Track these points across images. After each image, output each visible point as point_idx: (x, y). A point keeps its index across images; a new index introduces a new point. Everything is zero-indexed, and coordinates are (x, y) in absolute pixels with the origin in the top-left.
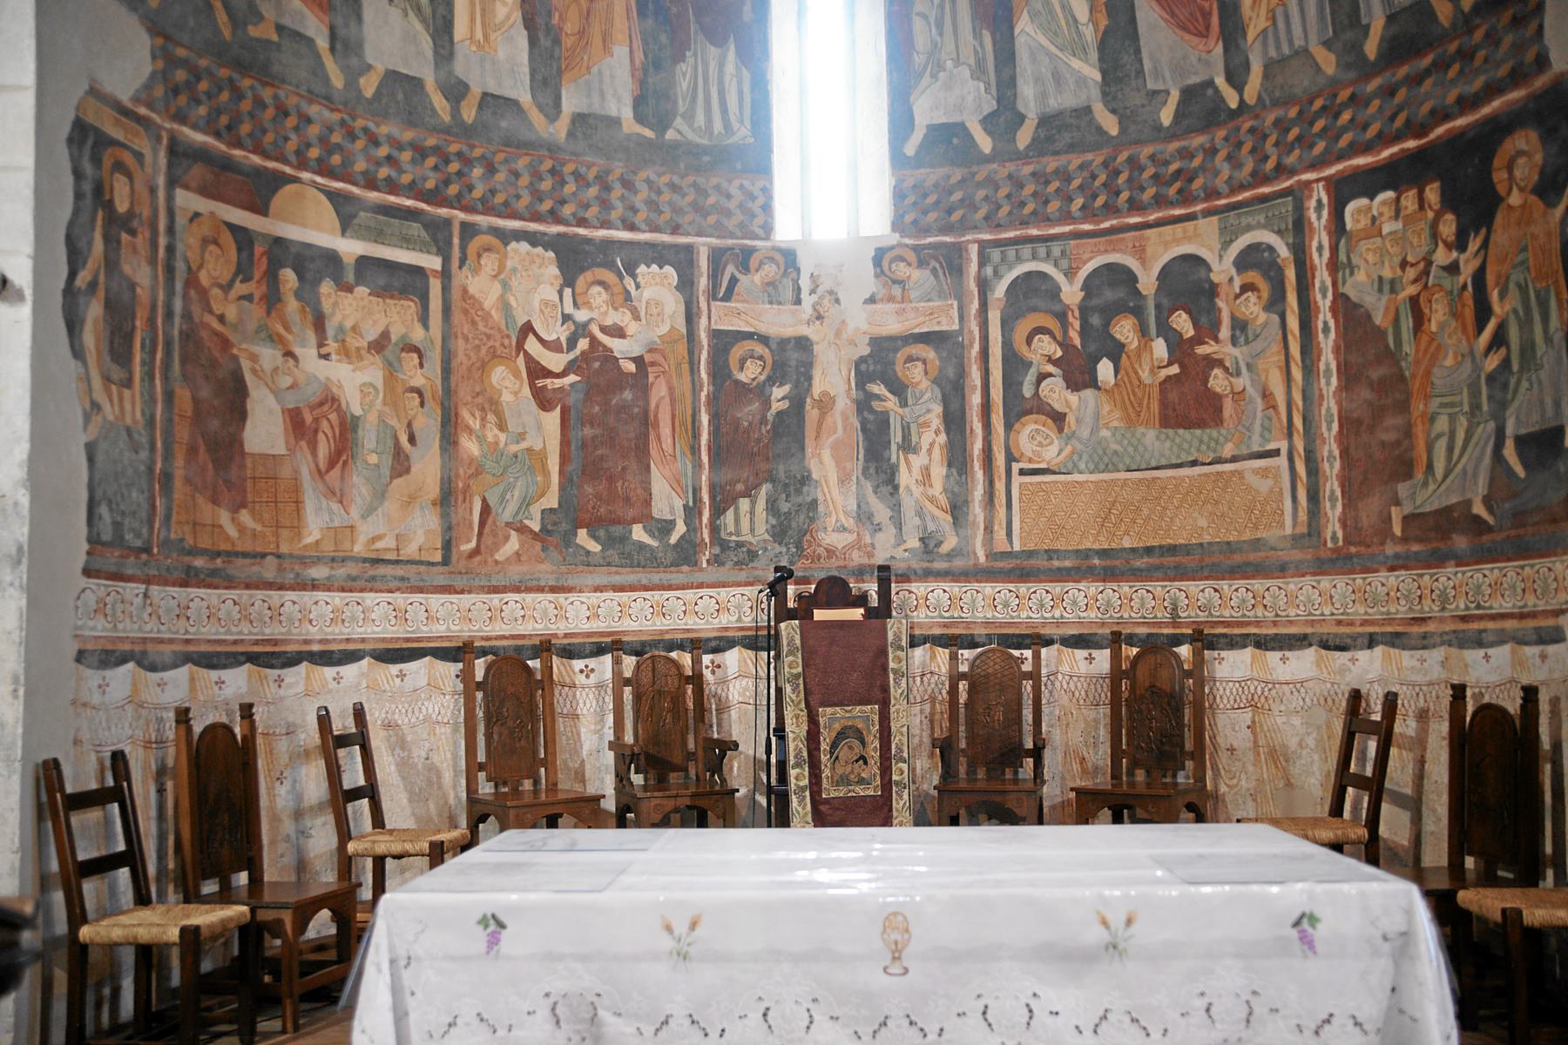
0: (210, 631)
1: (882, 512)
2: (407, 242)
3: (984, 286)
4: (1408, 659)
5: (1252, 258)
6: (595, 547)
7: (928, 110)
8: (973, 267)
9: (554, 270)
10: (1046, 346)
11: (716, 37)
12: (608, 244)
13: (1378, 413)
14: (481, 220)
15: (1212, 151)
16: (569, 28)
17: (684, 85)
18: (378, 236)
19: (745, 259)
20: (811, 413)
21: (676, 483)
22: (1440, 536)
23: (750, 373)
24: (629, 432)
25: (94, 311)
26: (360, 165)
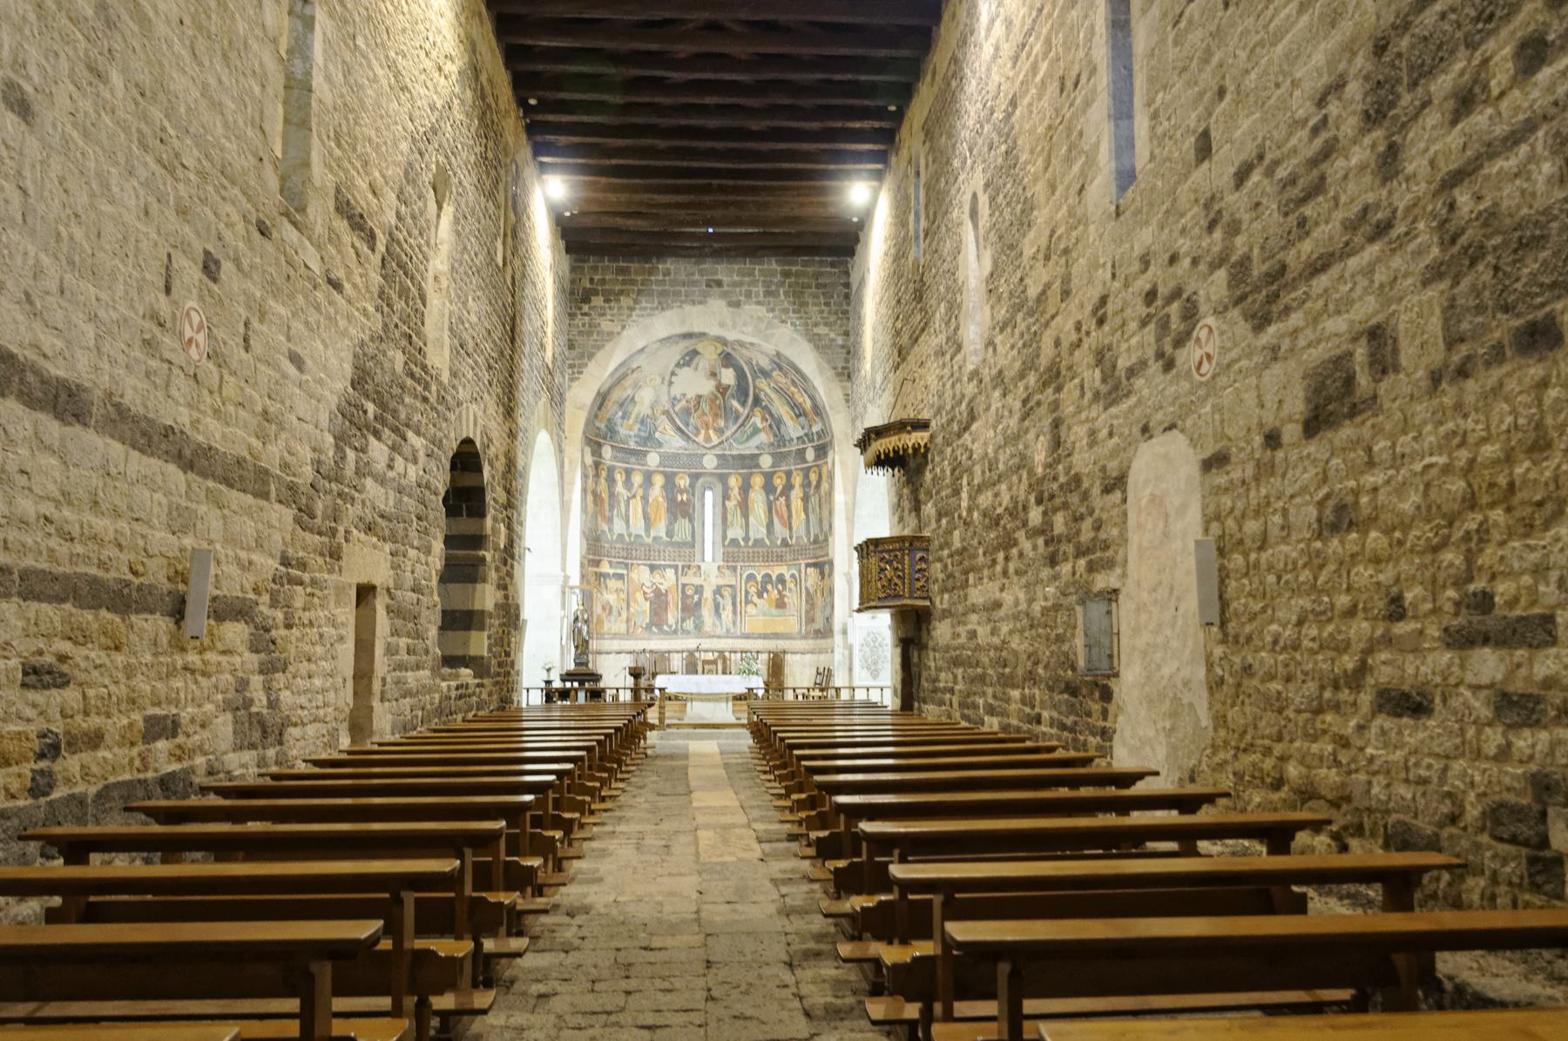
5: (793, 576)
7: (731, 534)
10: (753, 590)
23: (690, 592)
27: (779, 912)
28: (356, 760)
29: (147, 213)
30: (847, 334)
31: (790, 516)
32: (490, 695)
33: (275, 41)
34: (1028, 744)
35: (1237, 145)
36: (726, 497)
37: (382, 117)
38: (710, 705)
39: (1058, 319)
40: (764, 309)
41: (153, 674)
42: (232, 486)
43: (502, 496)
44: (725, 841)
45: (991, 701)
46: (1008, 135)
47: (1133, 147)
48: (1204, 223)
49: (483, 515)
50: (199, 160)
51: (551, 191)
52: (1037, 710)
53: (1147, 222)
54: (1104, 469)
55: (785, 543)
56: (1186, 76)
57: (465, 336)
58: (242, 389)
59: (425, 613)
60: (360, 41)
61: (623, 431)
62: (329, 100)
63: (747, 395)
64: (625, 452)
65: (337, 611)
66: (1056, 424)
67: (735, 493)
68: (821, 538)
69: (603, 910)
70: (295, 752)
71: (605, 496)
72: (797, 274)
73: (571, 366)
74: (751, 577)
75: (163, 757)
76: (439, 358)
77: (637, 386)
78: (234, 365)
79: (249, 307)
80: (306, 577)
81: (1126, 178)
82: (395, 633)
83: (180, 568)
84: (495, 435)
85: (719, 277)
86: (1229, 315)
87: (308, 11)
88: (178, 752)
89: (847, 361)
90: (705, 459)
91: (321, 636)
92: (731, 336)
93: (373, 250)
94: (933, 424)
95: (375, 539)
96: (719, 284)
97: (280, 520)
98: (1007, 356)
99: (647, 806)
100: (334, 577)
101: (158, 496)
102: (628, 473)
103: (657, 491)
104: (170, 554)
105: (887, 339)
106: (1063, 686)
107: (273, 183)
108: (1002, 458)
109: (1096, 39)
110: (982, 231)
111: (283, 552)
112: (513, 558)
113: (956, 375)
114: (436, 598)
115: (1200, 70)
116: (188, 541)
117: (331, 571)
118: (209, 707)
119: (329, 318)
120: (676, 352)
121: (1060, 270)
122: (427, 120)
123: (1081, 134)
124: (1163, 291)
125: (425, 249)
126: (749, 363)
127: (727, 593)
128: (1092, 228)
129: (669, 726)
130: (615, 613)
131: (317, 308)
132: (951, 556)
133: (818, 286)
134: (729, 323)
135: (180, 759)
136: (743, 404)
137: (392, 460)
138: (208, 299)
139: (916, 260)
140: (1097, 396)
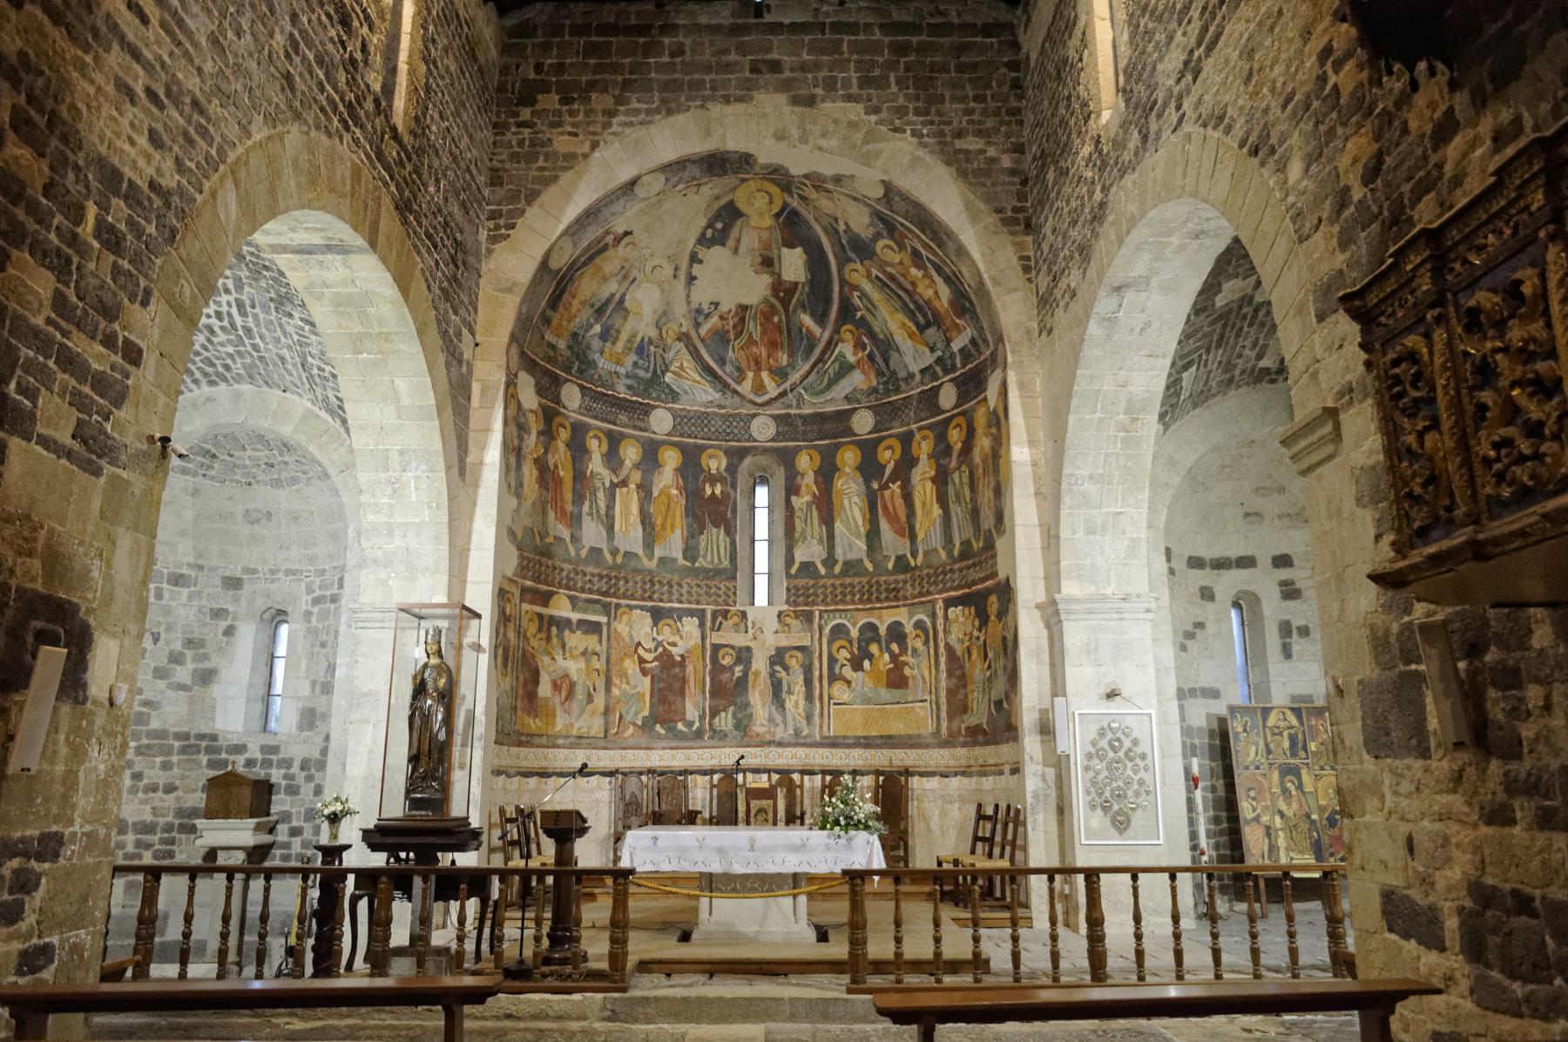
0: (525, 764)
1: (779, 719)
2: (595, 612)
3: (821, 628)
4: (965, 780)
5: (919, 625)
6: (662, 731)
7: (800, 555)
8: (817, 620)
9: (650, 620)
10: (844, 654)
11: (717, 525)
12: (671, 610)
13: (958, 687)
14: (623, 602)
15: (905, 582)
16: (659, 522)
17: (703, 544)
18: (585, 611)
19: (725, 614)
20: (751, 678)
21: (696, 705)
22: (977, 736)
23: (727, 661)
24: (677, 685)
25: (500, 652)
26: (580, 584)
30: (1019, 149)
31: (911, 514)
36: (792, 489)
38: (756, 904)
40: (860, 107)
61: (604, 364)
63: (828, 301)
64: (600, 398)
67: (808, 481)
71: (565, 473)
72: (921, 49)
73: (493, 216)
74: (839, 631)
77: (627, 277)
85: (775, 56)
89: (1022, 197)
92: (798, 163)
96: (775, 67)
102: (614, 441)
103: (667, 477)
127: (794, 662)
129: (645, 966)
130: (580, 695)
133: (960, 68)
134: (795, 133)
136: (821, 320)
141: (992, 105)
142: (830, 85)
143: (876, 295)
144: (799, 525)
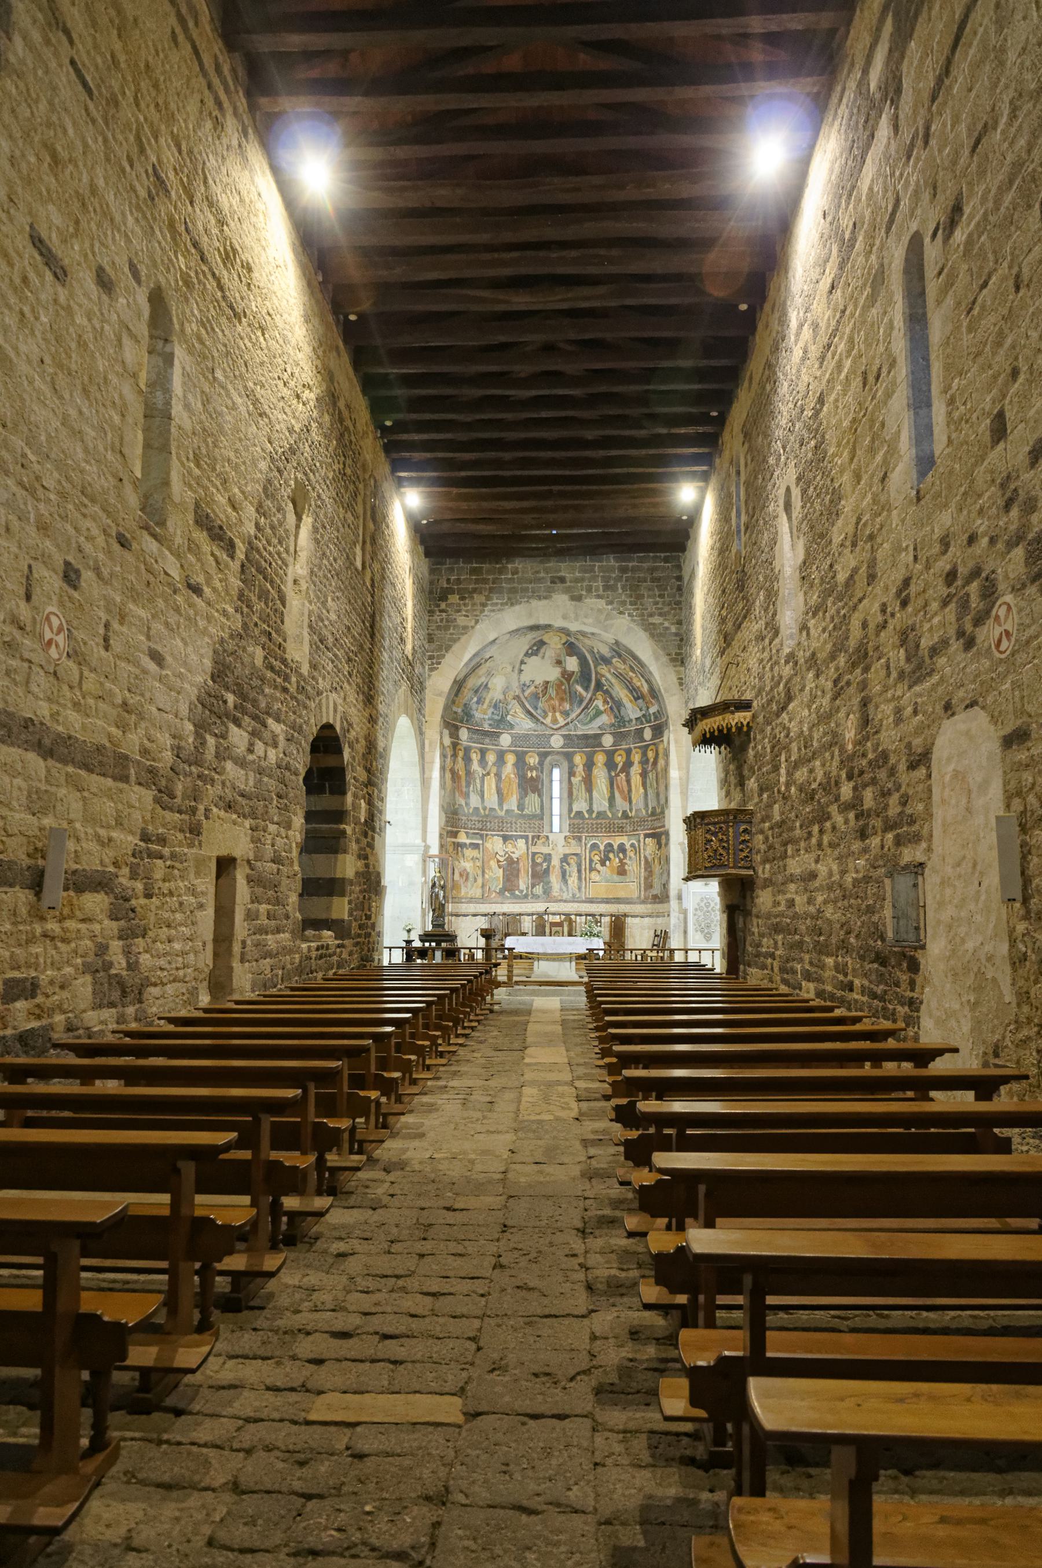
5: (632, 845)
7: (576, 808)
10: (597, 858)
23: (539, 861)
27: (583, 1175)
28: (213, 1018)
29: (8, 530)
30: (680, 623)
31: (630, 791)
32: (351, 954)
33: (135, 376)
34: (838, 1012)
35: (1032, 424)
37: (240, 440)
38: (556, 964)
39: (865, 601)
41: (12, 942)
42: (91, 771)
43: (363, 776)
44: (546, 1099)
45: (807, 967)
46: (817, 430)
47: (932, 434)
48: (1001, 502)
49: (344, 793)
50: (59, 482)
51: (407, 504)
52: (850, 977)
53: (946, 505)
54: (909, 745)
55: (625, 815)
56: (980, 360)
57: (324, 632)
58: (101, 684)
59: (285, 882)
60: (219, 374)
61: (478, 715)
62: (188, 425)
63: (590, 680)
65: (195, 882)
66: (865, 703)
67: (580, 769)
68: (658, 810)
69: (417, 1167)
70: (154, 1009)
71: (462, 773)
72: (634, 570)
73: (431, 658)
74: (594, 846)
75: (21, 1016)
76: (299, 652)
77: (490, 674)
78: (94, 663)
79: (108, 611)
80: (166, 851)
81: (925, 463)
82: (255, 900)
83: (40, 845)
84: (355, 720)
85: (562, 574)
86: (1027, 592)
87: (168, 349)
88: (37, 1012)
89: (680, 647)
90: (553, 739)
91: (181, 904)
92: (574, 627)
93: (232, 558)
94: (755, 704)
95: (234, 816)
96: (562, 580)
97: (139, 800)
98: (819, 640)
99: (483, 1061)
100: (194, 851)
101: (18, 781)
103: (509, 769)
104: (30, 833)
105: (714, 627)
106: (873, 955)
107: (133, 500)
108: (816, 736)
109: (895, 333)
110: (795, 523)
111: (143, 829)
112: (373, 830)
113: (774, 658)
114: (297, 868)
115: (994, 354)
116: (47, 821)
117: (191, 845)
118: (68, 970)
119: (188, 619)
120: (524, 643)
121: (866, 555)
122: (286, 440)
123: (883, 425)
124: (963, 571)
125: (284, 555)
126: (591, 652)
127: (572, 861)
128: (895, 512)
129: (517, 983)
130: (471, 878)
131: (177, 610)
132: (771, 828)
133: (653, 580)
134: (572, 615)
135: (39, 1017)
136: (586, 689)
137: (252, 744)
138: (69, 605)
139: (738, 552)
140: (901, 675)
141: (667, 599)
142: (589, 590)
143: (613, 681)
144: (575, 792)
